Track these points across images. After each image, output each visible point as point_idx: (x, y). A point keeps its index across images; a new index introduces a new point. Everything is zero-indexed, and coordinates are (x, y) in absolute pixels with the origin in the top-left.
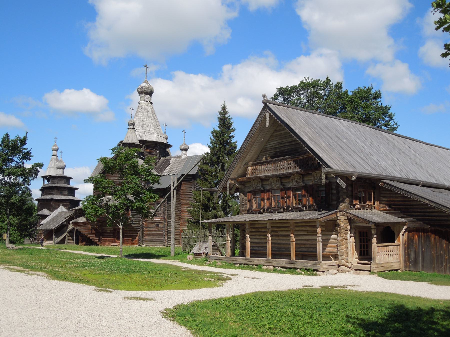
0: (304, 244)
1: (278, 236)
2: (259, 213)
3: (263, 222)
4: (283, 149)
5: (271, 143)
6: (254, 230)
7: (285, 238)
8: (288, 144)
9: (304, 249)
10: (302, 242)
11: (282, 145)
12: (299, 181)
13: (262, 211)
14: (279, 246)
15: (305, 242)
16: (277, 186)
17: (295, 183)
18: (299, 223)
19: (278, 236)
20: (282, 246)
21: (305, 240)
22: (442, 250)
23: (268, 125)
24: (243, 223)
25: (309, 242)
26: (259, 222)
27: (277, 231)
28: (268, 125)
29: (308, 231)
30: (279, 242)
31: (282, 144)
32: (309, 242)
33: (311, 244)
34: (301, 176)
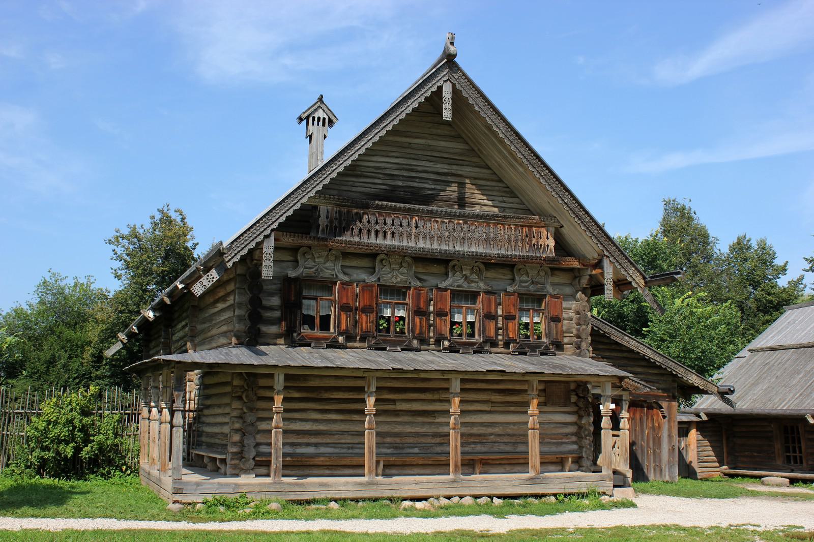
0: (480, 435)
1: (396, 413)
2: (329, 347)
3: (439, 376)
4: (416, 185)
5: (375, 159)
6: (297, 395)
7: (420, 419)
8: (433, 176)
9: (479, 448)
10: (475, 430)
11: (414, 174)
12: (474, 277)
13: (341, 339)
14: (398, 440)
15: (482, 430)
16: (401, 278)
17: (460, 282)
18: (473, 383)
19: (396, 413)
20: (411, 440)
21: (482, 424)
22: (643, 439)
23: (447, 115)
24: (360, 374)
25: (497, 430)
26: (423, 376)
27: (394, 401)
28: (447, 115)
29: (492, 402)
30: (398, 429)
31: (412, 170)
32: (497, 430)
33: (499, 435)
34: (482, 266)
